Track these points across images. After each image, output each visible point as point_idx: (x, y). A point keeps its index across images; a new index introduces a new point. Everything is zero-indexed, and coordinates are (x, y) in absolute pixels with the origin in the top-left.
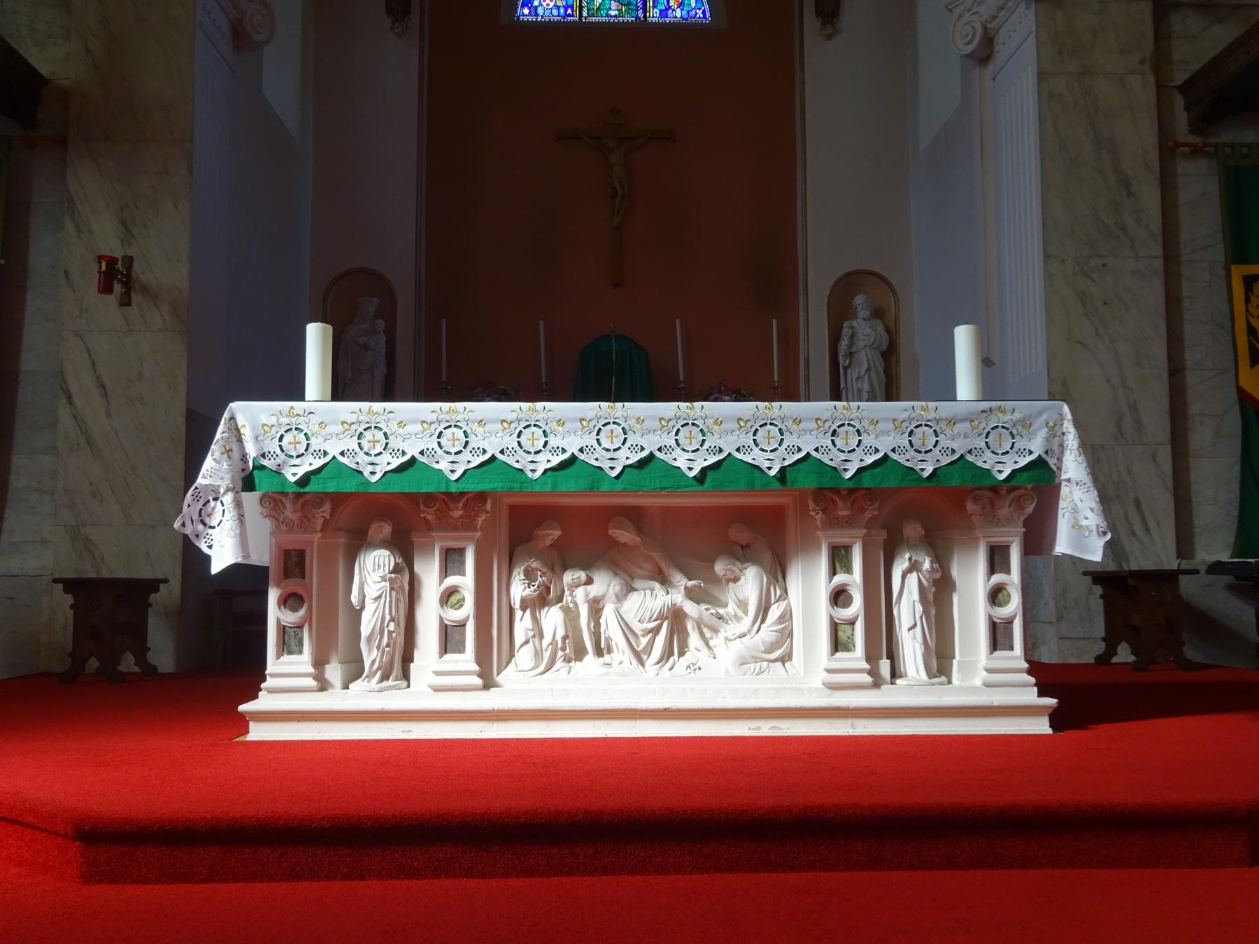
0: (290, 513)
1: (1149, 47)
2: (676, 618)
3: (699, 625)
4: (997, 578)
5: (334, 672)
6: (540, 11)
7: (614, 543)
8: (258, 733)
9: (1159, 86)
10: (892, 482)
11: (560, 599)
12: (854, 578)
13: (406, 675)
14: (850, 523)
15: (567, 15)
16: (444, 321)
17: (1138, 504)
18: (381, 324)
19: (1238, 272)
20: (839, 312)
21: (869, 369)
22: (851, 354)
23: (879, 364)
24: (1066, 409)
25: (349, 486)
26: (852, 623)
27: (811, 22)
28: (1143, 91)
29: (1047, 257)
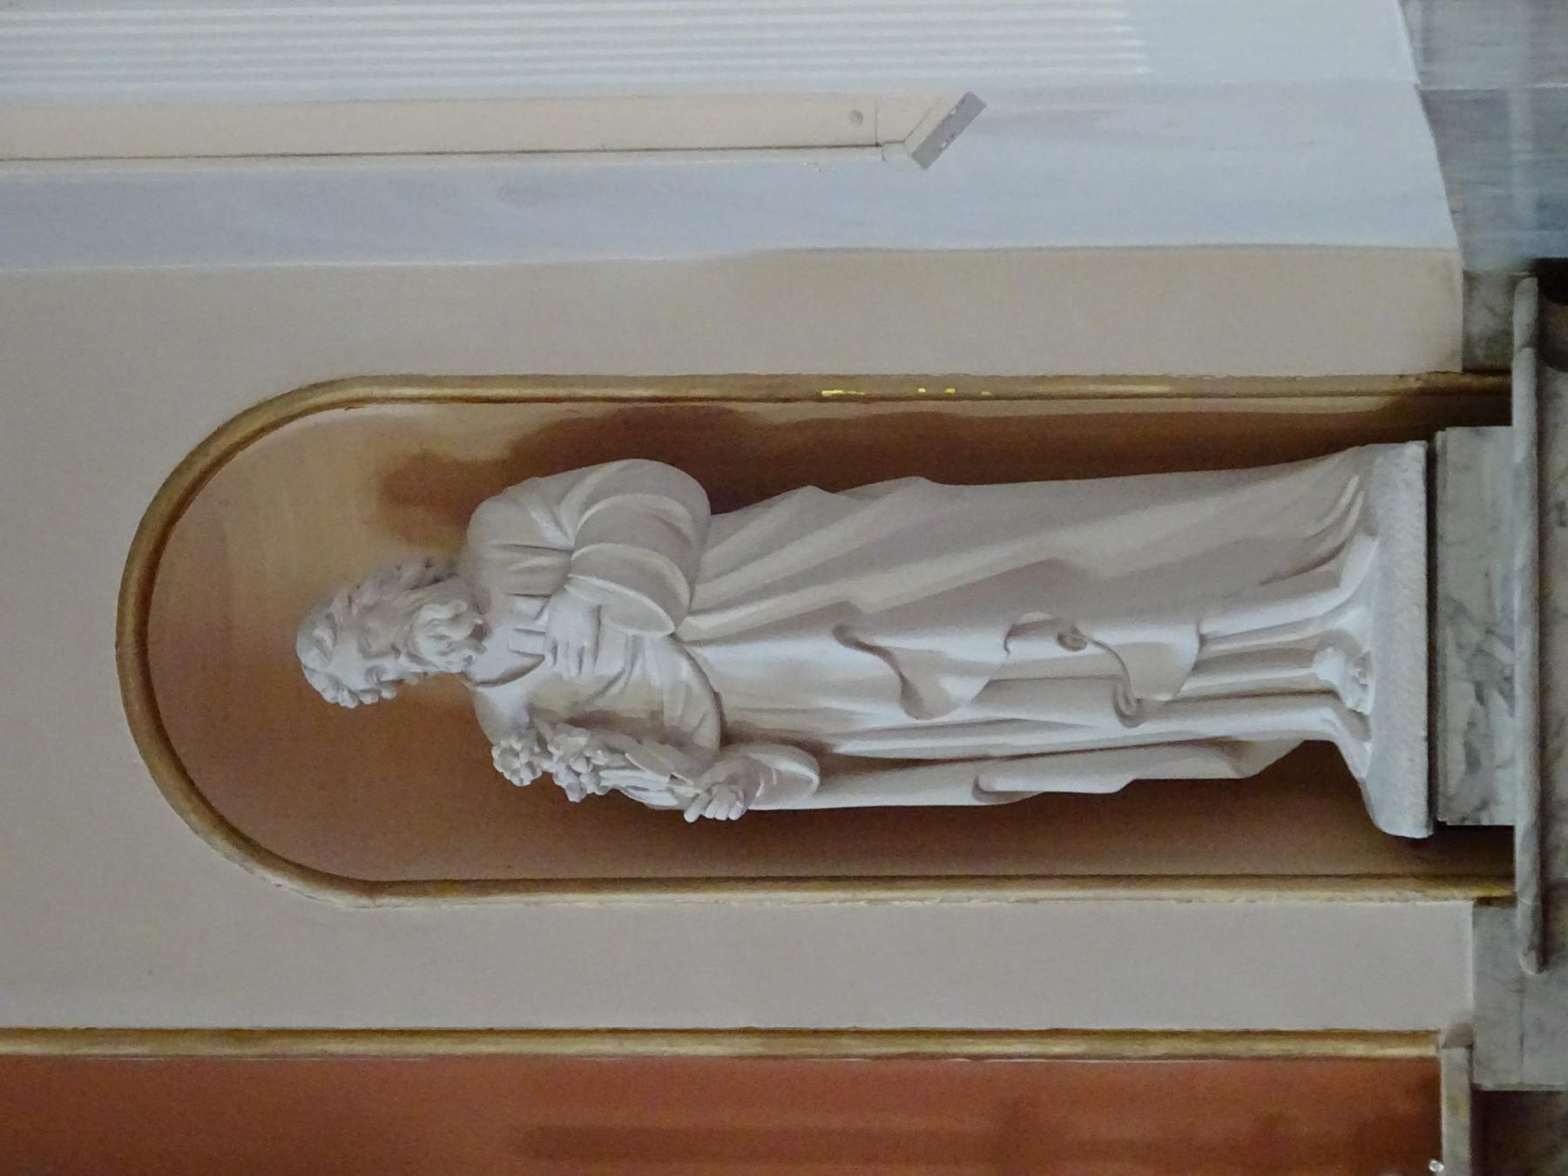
22: (729, 738)
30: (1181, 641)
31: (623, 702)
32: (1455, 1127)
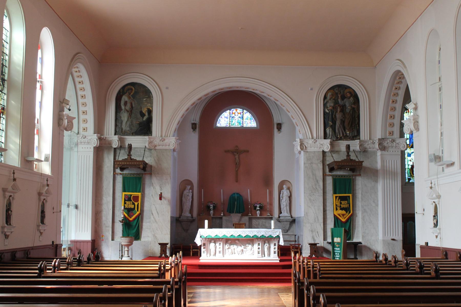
0: (204, 239)
1: (322, 159)
2: (242, 250)
3: (245, 251)
4: (275, 247)
5: (208, 255)
6: (221, 125)
7: (236, 243)
10: (263, 237)
11: (230, 248)
12: (260, 247)
13: (215, 256)
14: (260, 241)
15: (227, 125)
16: (203, 190)
17: (318, 232)
18: (191, 191)
19: (335, 195)
20: (281, 188)
21: (286, 200)
22: (282, 197)
23: (288, 199)
24: (281, 230)
25: (211, 237)
26: (260, 251)
27: (276, 130)
28: (321, 166)
29: (304, 193)
30: (285, 209)
31: (283, 194)
32: (272, 217)
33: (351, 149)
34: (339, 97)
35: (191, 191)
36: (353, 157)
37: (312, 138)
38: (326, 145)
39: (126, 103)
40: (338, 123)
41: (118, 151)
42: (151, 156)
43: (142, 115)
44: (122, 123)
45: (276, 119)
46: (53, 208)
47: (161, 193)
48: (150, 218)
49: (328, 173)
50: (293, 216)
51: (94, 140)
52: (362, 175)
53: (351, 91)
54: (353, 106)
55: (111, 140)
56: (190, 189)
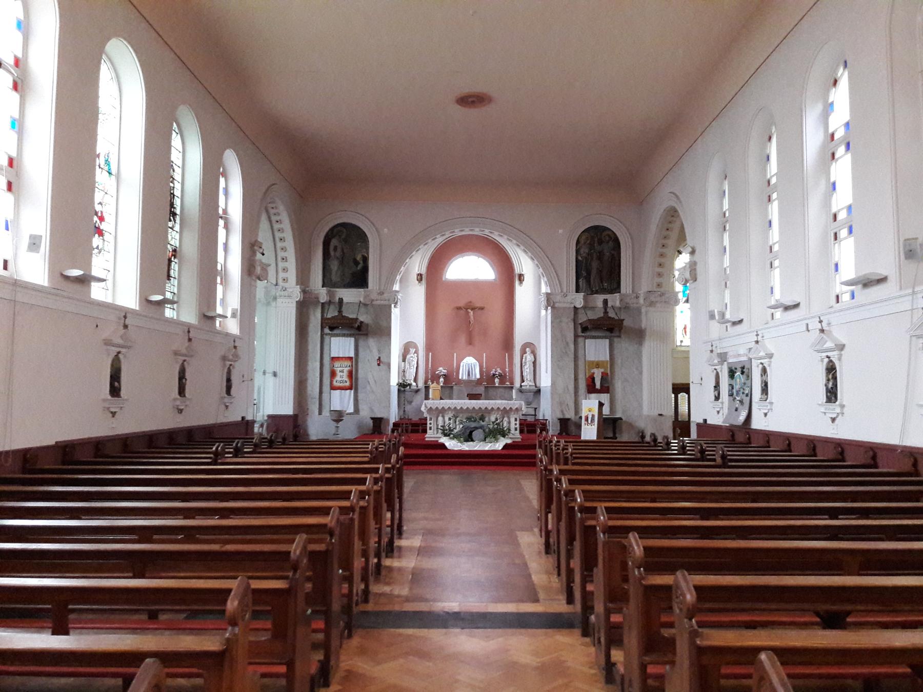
8: (427, 439)
9: (574, 323)
18: (416, 355)
20: (523, 352)
23: (532, 365)
27: (517, 282)
28: (572, 325)
33: (610, 304)
34: (594, 241)
35: (416, 355)
36: (612, 314)
37: (562, 292)
38: (579, 300)
39: (335, 248)
40: (594, 272)
41: (327, 306)
42: (367, 313)
43: (356, 263)
44: (331, 274)
45: (517, 271)
46: (243, 376)
47: (379, 357)
48: (365, 387)
49: (580, 333)
50: (538, 385)
51: (296, 293)
52: (622, 336)
53: (610, 233)
54: (613, 252)
55: (318, 294)
56: (415, 353)
